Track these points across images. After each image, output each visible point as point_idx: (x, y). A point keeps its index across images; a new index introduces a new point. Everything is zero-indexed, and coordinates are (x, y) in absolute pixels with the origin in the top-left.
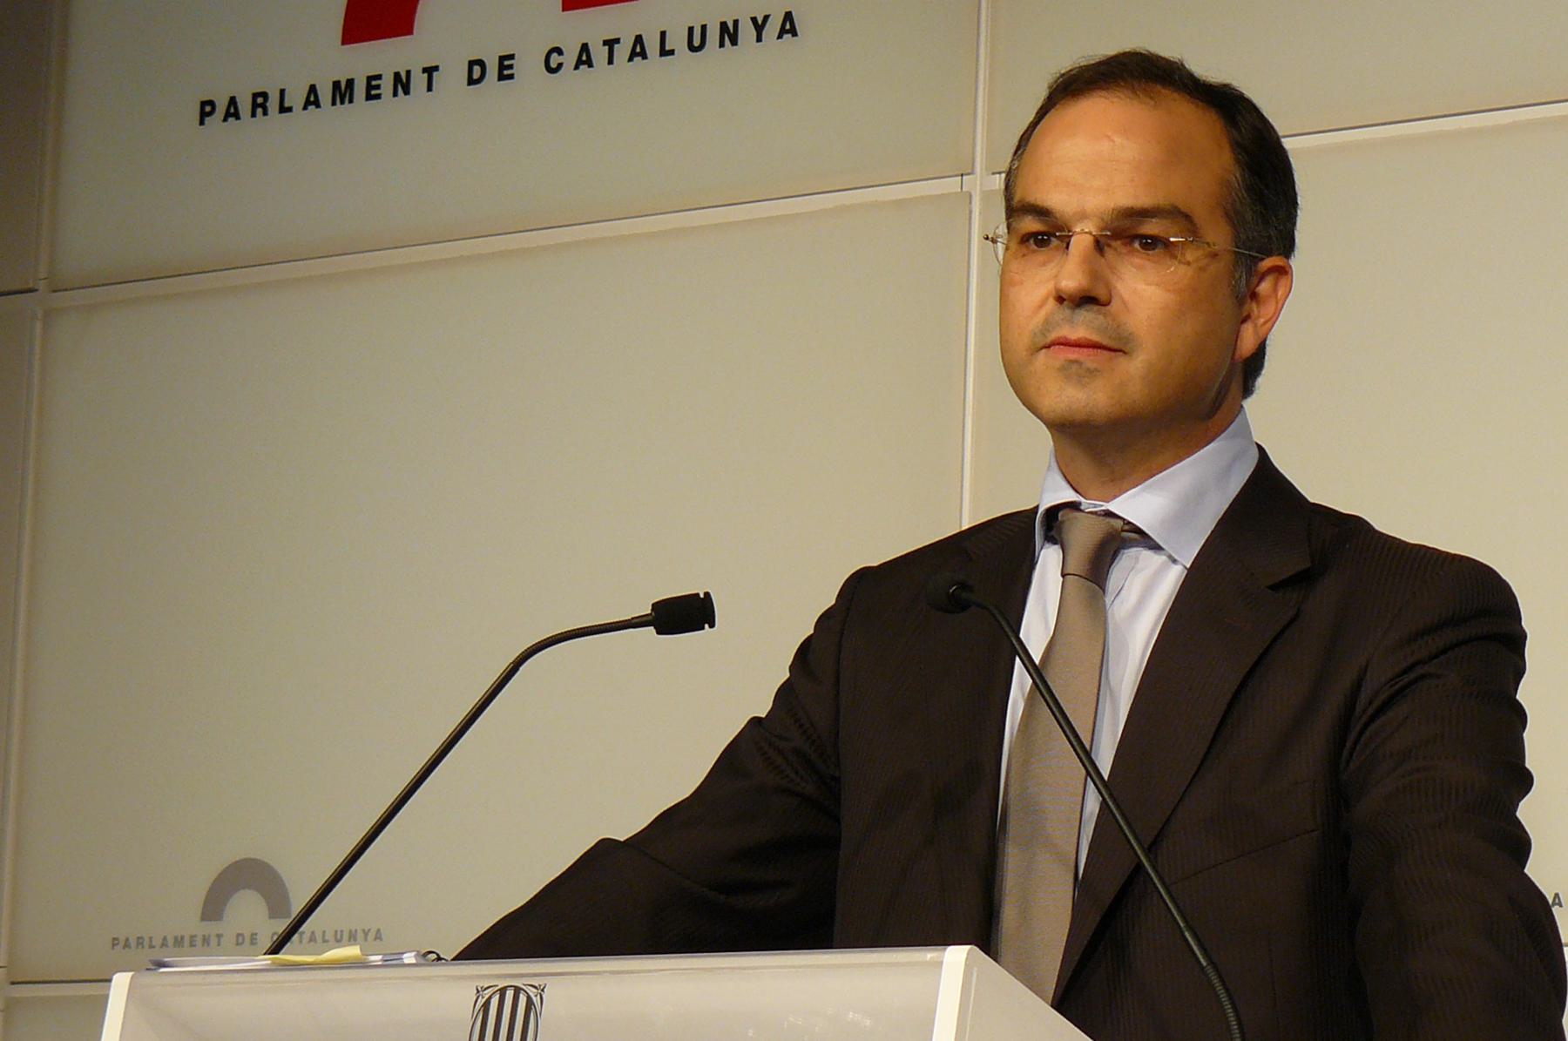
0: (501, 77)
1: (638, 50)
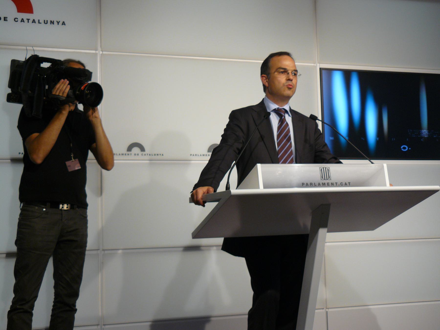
0: (5, 20)
1: (34, 21)
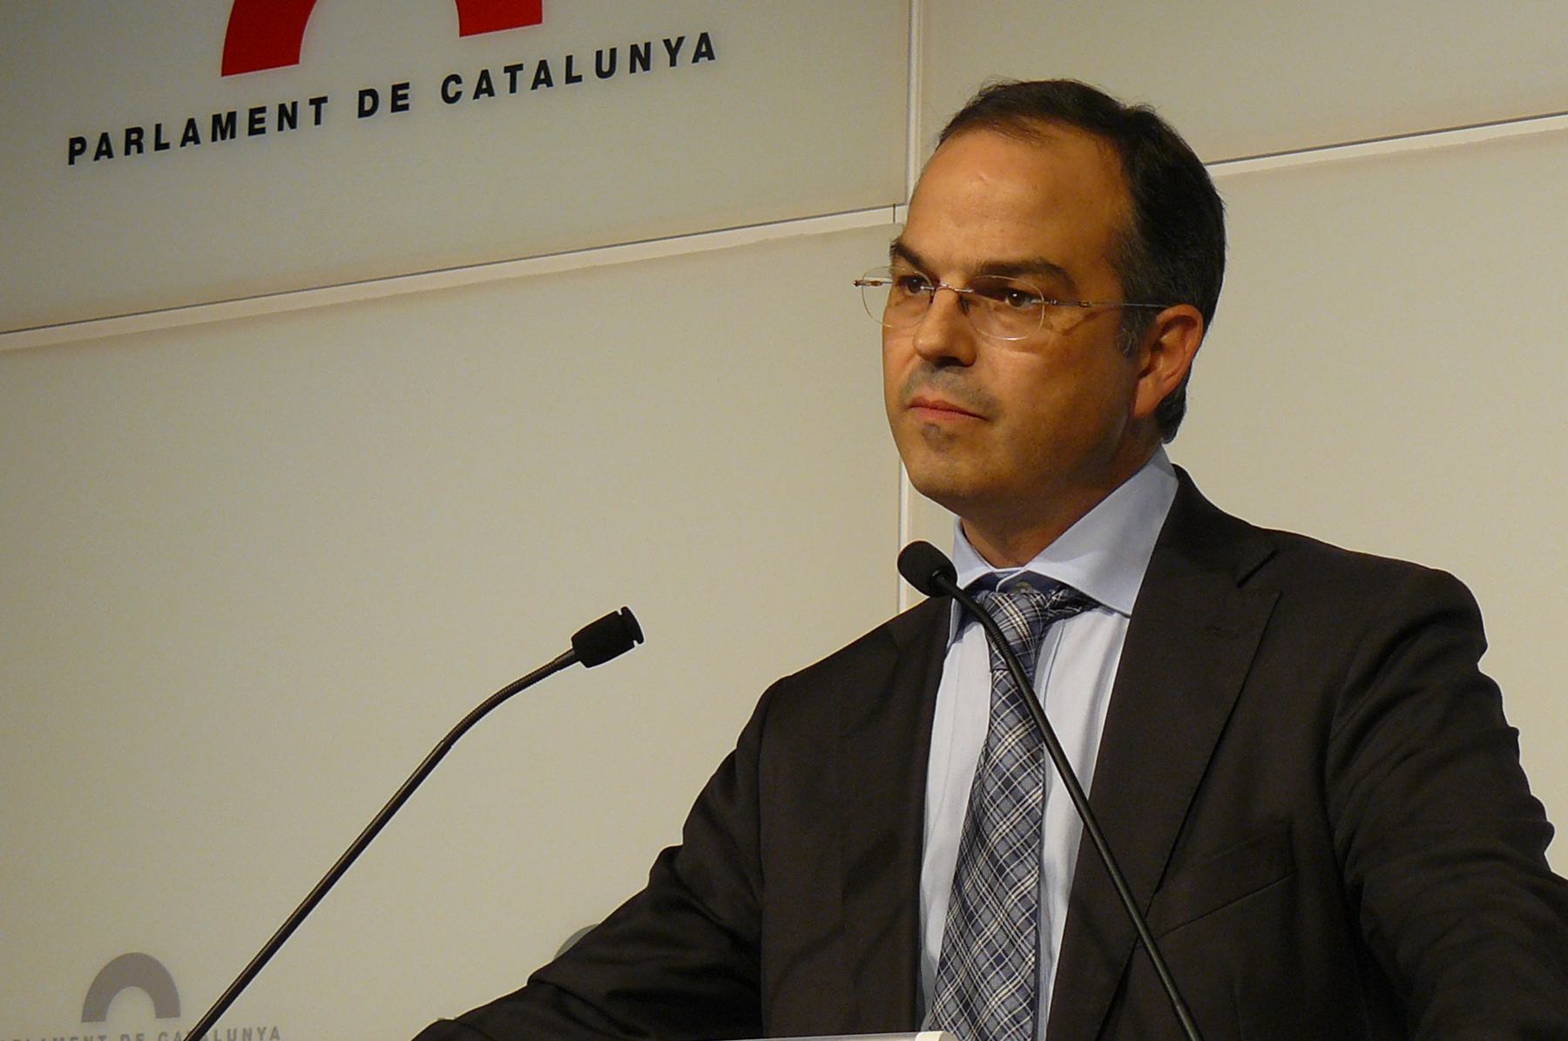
0: (395, 108)
1: (543, 77)
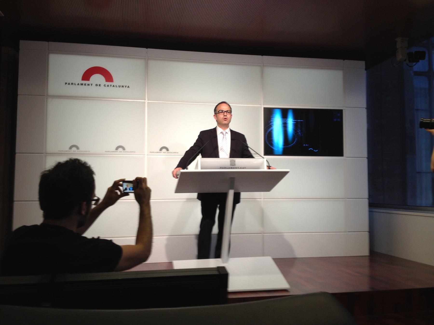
1: (114, 86)
